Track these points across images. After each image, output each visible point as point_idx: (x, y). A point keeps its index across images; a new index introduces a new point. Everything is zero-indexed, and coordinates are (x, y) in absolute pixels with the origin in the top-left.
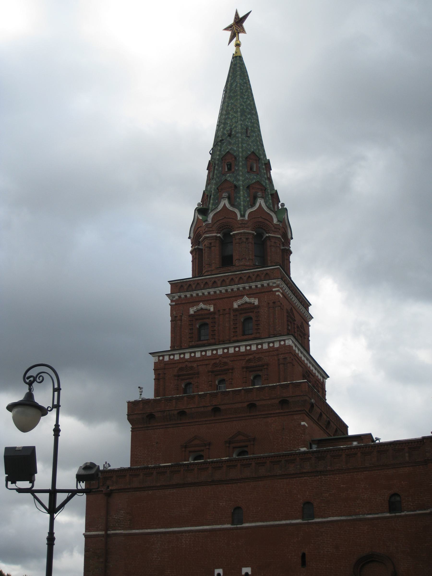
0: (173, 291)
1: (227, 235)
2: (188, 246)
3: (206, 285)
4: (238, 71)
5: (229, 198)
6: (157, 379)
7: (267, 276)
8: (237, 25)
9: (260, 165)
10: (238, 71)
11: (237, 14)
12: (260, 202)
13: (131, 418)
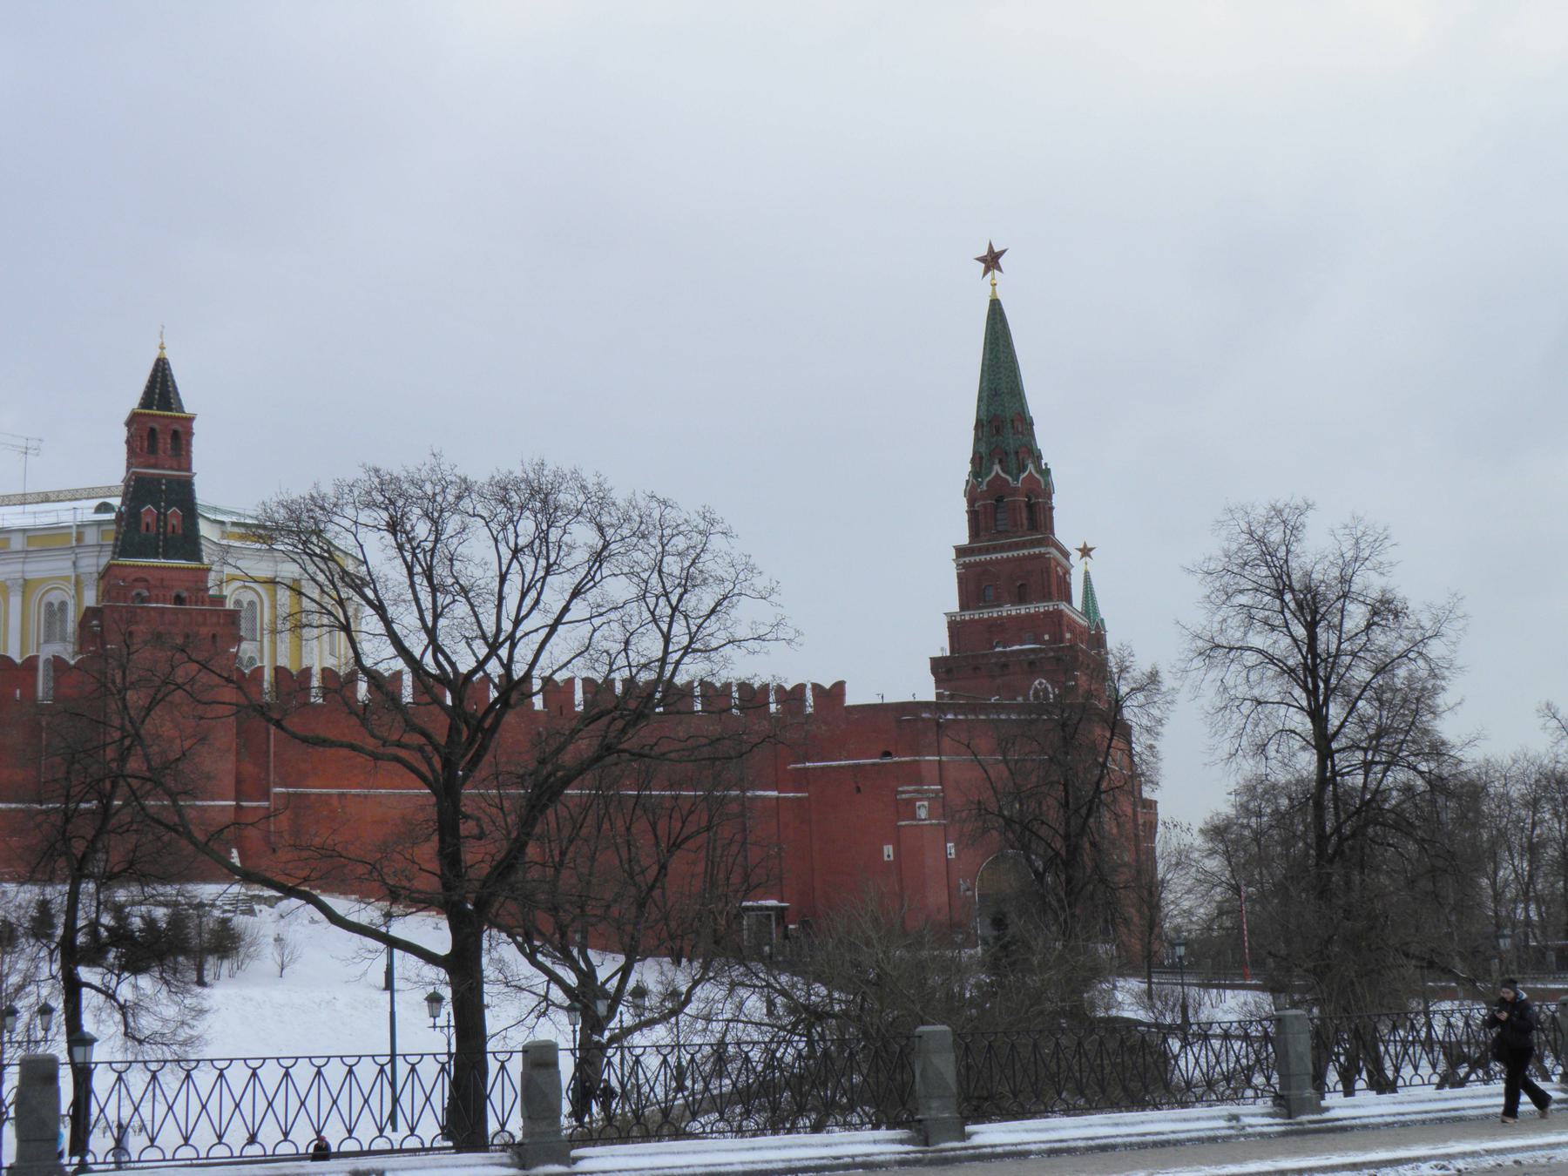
0: (958, 556)
1: (999, 500)
2: (963, 505)
3: (988, 551)
4: (996, 314)
5: (1000, 462)
6: (951, 637)
7: (1039, 543)
8: (992, 261)
9: (1024, 423)
10: (996, 314)
11: (991, 246)
12: (1031, 467)
13: (934, 670)
